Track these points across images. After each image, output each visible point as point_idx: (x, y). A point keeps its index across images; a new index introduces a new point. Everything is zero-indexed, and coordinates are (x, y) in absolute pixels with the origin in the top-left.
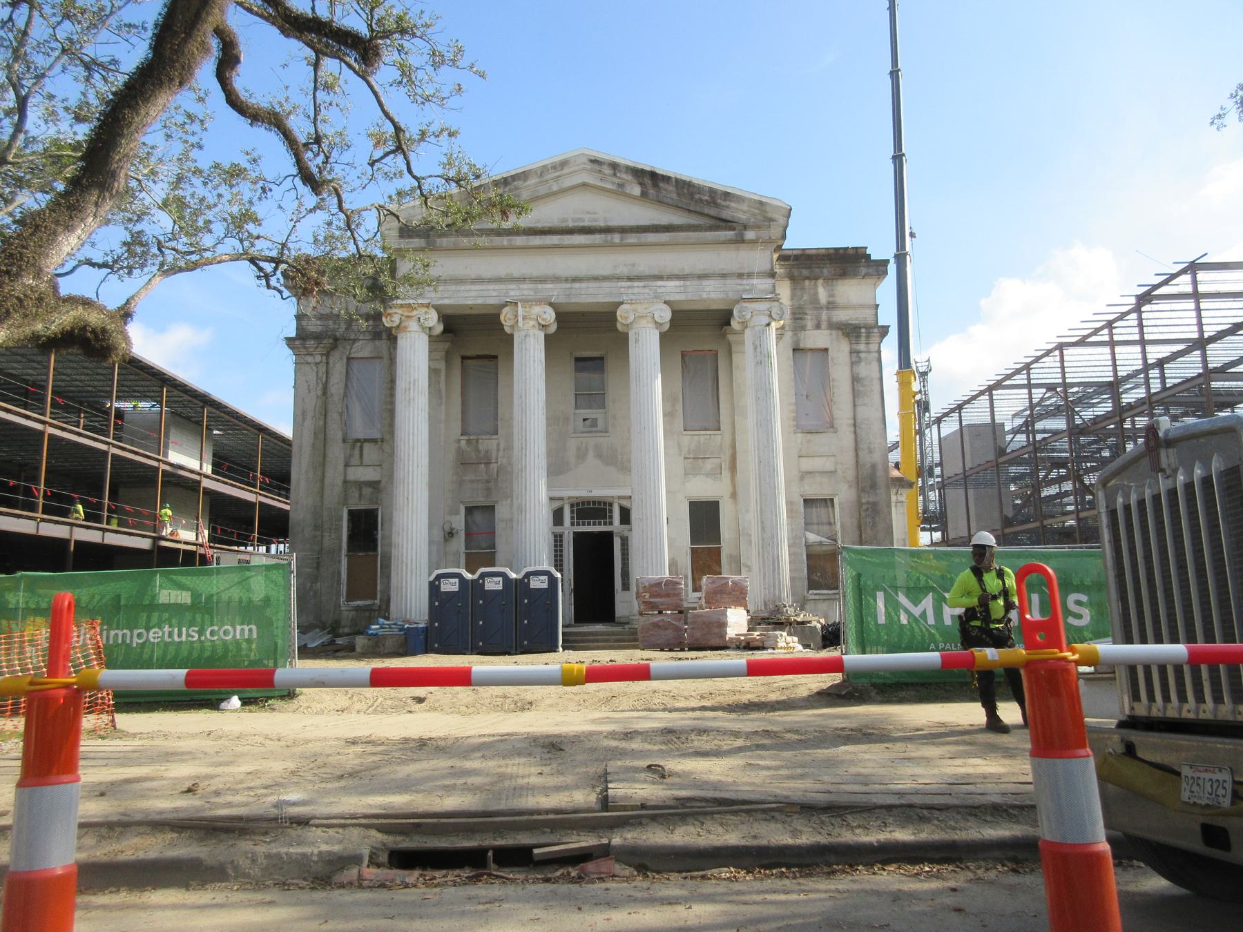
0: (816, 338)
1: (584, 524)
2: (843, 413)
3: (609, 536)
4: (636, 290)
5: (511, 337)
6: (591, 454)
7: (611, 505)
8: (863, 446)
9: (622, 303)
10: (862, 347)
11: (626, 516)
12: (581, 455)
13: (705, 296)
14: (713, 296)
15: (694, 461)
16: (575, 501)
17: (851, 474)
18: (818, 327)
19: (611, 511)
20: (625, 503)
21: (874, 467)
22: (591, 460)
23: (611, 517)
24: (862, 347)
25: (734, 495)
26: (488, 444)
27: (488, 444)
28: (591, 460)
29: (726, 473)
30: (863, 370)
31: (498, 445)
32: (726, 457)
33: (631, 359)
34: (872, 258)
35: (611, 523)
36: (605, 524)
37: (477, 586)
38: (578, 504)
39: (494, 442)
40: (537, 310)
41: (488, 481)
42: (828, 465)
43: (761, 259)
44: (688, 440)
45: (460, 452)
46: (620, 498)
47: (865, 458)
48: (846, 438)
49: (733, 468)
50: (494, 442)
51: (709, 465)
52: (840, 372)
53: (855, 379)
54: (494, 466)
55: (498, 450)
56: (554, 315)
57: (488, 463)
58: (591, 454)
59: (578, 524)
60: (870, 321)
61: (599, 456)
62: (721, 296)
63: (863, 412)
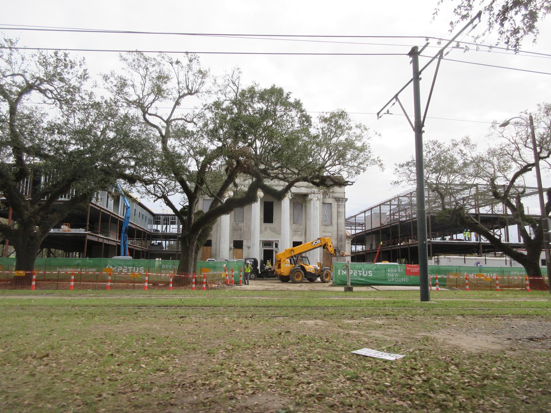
0: (329, 200)
2: (334, 221)
3: (272, 250)
6: (268, 229)
8: (339, 230)
10: (340, 204)
11: (277, 246)
12: (266, 229)
15: (295, 232)
17: (336, 237)
18: (329, 197)
20: (277, 242)
21: (342, 235)
22: (268, 230)
24: (340, 204)
26: (241, 225)
27: (241, 225)
28: (268, 230)
29: (303, 236)
30: (340, 210)
32: (304, 231)
42: (330, 234)
44: (293, 226)
45: (233, 227)
47: (339, 233)
48: (335, 228)
49: (305, 234)
51: (299, 233)
52: (334, 210)
53: (338, 212)
54: (242, 231)
58: (268, 229)
60: (343, 197)
61: (270, 229)
63: (339, 221)
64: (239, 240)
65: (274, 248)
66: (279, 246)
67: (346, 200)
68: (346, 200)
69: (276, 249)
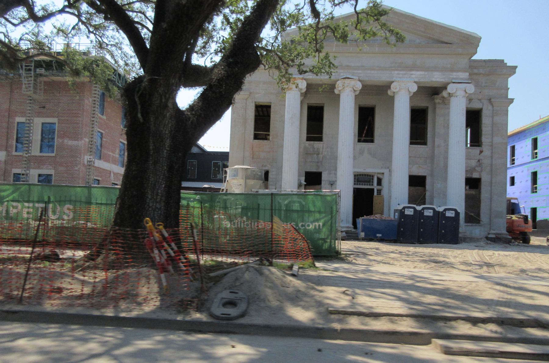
1: (360, 184)
4: (401, 76)
5: (339, 96)
7: (373, 176)
9: (393, 82)
12: (361, 152)
13: (434, 80)
14: (438, 80)
16: (357, 174)
19: (373, 179)
20: (380, 176)
23: (373, 182)
25: (432, 175)
31: (323, 146)
33: (395, 109)
34: (508, 65)
35: (372, 185)
36: (370, 185)
37: (421, 213)
38: (358, 175)
39: (321, 145)
40: (352, 83)
41: (318, 162)
43: (463, 62)
46: (378, 173)
50: (321, 145)
54: (321, 156)
55: (323, 148)
56: (361, 86)
57: (318, 154)
59: (357, 184)
62: (443, 80)
64: (314, 170)
65: (375, 187)
66: (385, 182)
67: (512, 101)
68: (512, 101)
69: (379, 187)
